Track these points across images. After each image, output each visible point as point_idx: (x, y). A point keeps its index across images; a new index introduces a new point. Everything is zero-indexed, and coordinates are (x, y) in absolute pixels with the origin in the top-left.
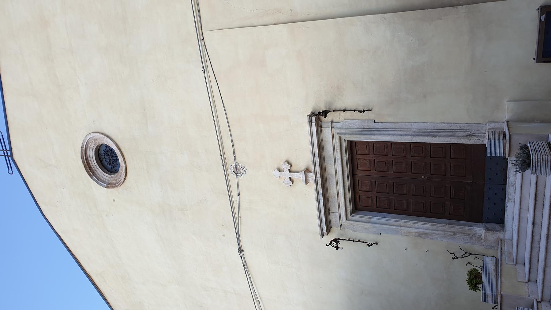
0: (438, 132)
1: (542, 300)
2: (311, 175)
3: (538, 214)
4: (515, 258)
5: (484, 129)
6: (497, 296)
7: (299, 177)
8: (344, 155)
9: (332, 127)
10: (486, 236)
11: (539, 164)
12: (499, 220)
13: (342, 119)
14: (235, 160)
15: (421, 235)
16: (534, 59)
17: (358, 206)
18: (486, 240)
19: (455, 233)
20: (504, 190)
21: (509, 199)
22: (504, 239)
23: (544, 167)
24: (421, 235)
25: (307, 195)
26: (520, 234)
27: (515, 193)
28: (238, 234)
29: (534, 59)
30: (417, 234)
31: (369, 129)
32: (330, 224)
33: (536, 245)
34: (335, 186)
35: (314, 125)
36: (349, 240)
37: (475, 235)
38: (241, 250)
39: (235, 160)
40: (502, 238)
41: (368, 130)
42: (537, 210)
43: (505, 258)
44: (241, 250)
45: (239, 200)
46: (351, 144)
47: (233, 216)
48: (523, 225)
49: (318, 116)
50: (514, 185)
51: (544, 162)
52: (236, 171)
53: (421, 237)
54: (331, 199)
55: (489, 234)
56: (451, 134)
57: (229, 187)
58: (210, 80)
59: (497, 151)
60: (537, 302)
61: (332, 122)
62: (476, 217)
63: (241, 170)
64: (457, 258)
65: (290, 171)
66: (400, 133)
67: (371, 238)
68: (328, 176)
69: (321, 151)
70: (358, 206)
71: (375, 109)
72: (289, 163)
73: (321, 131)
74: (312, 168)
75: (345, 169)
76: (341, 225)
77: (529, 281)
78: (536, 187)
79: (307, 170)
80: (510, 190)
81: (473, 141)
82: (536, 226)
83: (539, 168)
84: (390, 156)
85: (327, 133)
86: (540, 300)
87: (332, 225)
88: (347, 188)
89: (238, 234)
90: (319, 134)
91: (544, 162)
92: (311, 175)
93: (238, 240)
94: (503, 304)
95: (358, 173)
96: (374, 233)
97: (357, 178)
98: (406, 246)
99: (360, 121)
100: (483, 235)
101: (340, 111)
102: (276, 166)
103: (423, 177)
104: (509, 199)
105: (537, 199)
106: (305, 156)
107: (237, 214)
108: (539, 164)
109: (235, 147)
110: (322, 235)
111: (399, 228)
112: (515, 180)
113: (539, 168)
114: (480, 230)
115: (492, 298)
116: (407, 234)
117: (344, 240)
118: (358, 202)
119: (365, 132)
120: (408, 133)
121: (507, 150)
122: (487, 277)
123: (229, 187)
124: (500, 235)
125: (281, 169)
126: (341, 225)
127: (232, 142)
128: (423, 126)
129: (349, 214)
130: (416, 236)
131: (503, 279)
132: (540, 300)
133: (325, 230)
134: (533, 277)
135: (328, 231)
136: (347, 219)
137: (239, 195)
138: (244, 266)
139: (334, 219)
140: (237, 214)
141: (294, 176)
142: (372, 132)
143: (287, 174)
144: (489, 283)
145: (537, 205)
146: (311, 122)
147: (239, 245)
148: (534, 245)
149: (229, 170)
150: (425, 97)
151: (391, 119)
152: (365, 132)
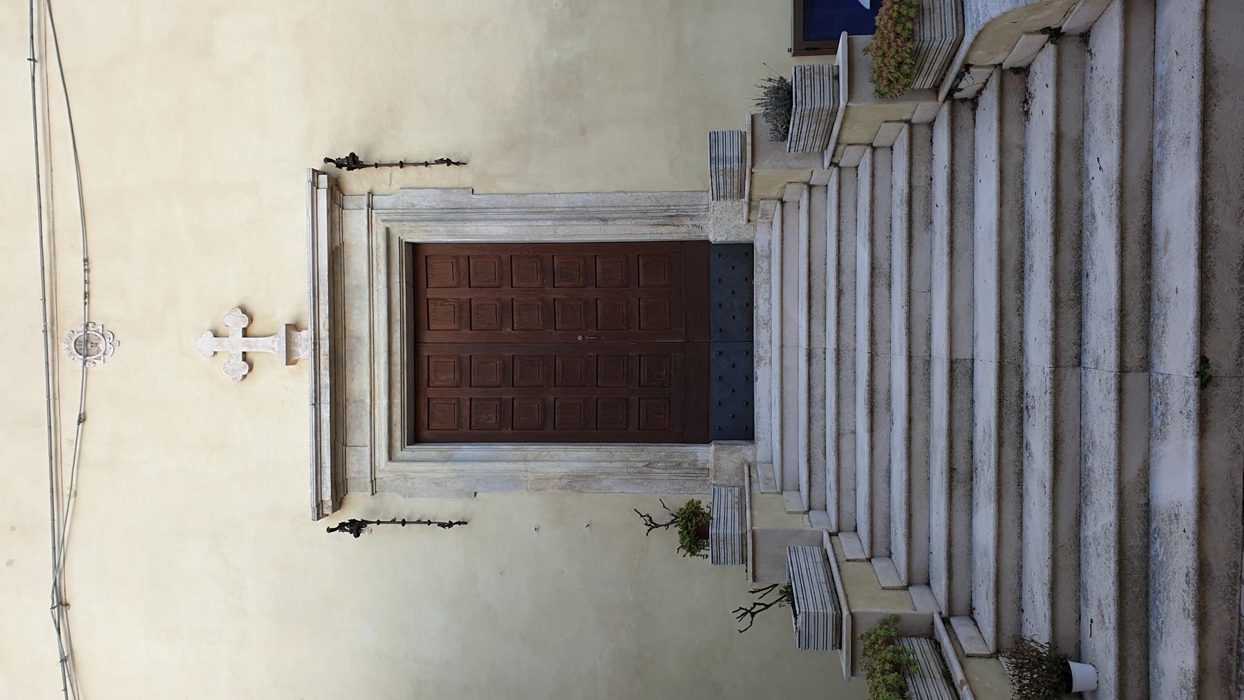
0: (611, 213)
1: (839, 530)
2: (304, 338)
3: (817, 329)
4: (778, 475)
5: (705, 202)
6: (743, 537)
7: (269, 348)
8: (396, 279)
9: (370, 206)
10: (717, 458)
11: (808, 82)
12: (746, 433)
13: (396, 187)
14: (87, 314)
15: (578, 482)
16: (790, 50)
17: (422, 425)
18: (717, 469)
19: (649, 465)
20: (750, 329)
21: (761, 359)
22: (756, 463)
23: (818, 96)
24: (578, 482)
25: (287, 400)
26: (786, 412)
27: (770, 342)
28: (59, 547)
29: (790, 50)
30: (564, 482)
31: (459, 209)
32: (345, 481)
33: (816, 410)
34: (366, 369)
35: (323, 196)
36: (393, 521)
37: (694, 463)
38: (61, 604)
39: (87, 314)
40: (750, 460)
41: (457, 213)
42: (813, 321)
43: (759, 487)
44: (61, 604)
45: (79, 439)
46: (414, 250)
47: (54, 490)
48: (789, 387)
49: (337, 176)
50: (768, 324)
51: (817, 77)
52: (85, 347)
53: (573, 488)
54: (351, 409)
55: (725, 455)
56: (637, 215)
57: (52, 399)
58: (46, 99)
59: (728, 154)
60: (831, 535)
61: (371, 194)
62: (697, 431)
63: (102, 346)
64: (657, 526)
65: (245, 333)
66: (530, 216)
67: (449, 509)
68: (350, 342)
69: (337, 269)
70: (422, 425)
71: (475, 162)
72: (244, 311)
73: (341, 218)
74: (308, 322)
75: (397, 316)
76: (373, 481)
77: (810, 509)
78: (810, 264)
79: (293, 328)
80: (760, 336)
81: (683, 229)
82: (814, 361)
83: (808, 90)
84: (507, 287)
85: (355, 222)
86: (834, 529)
87: (351, 484)
88: (397, 369)
89: (59, 547)
90: (335, 226)
91: (817, 77)
92: (304, 338)
93: (58, 569)
94: (759, 558)
95: (428, 337)
96: (459, 494)
97: (425, 352)
98: (538, 513)
99: (438, 192)
100: (711, 459)
101: (391, 165)
102: (208, 325)
103: (580, 338)
104: (761, 359)
105: (813, 294)
106: (291, 291)
107: (67, 484)
108: (808, 82)
109: (93, 275)
110: (320, 514)
111: (521, 466)
112: (770, 310)
113: (808, 90)
114: (705, 453)
115: (733, 546)
116: (541, 485)
117: (378, 522)
118: (424, 417)
119: (451, 216)
120: (548, 216)
121: (749, 148)
122: (724, 526)
123: (52, 399)
124: (744, 451)
125: (222, 330)
126: (373, 481)
127: (86, 260)
128: (578, 200)
129: (397, 444)
130: (563, 488)
131: (756, 513)
132: (834, 529)
133: (327, 495)
134: (816, 502)
135: (338, 503)
136: (390, 459)
137: (82, 420)
138: (63, 660)
139: (357, 464)
140: (67, 484)
141: (255, 346)
142: (469, 216)
143: (237, 343)
144: (726, 519)
145: (813, 309)
146: (315, 185)
147: (57, 589)
148: (814, 411)
149: (63, 346)
150: (583, 132)
151: (509, 187)
152: (451, 216)
